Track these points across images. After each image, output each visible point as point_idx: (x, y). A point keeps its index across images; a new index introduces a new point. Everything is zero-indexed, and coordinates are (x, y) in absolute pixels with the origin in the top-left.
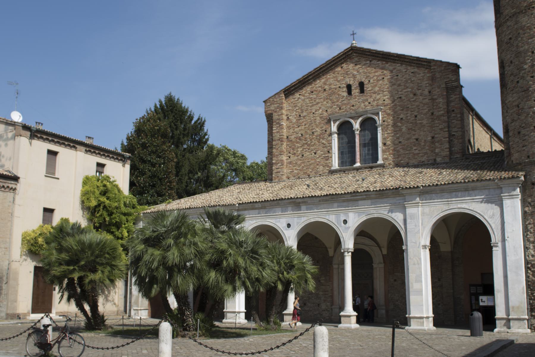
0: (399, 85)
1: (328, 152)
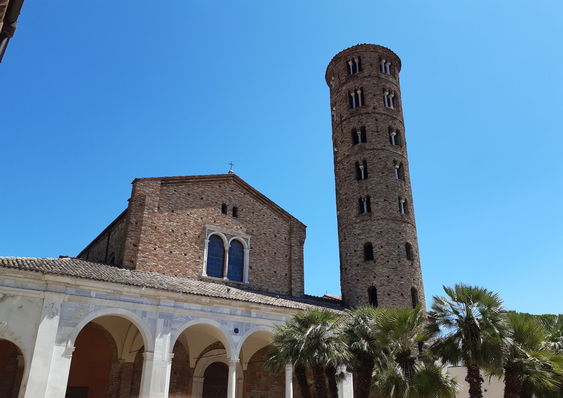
0: (265, 224)
1: (200, 258)
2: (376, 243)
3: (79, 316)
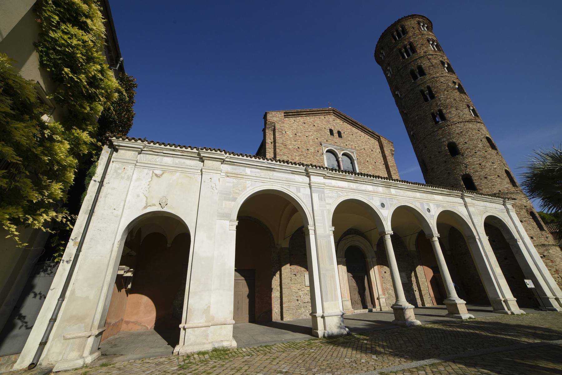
0: (362, 142)
2: (460, 142)
3: (238, 191)
